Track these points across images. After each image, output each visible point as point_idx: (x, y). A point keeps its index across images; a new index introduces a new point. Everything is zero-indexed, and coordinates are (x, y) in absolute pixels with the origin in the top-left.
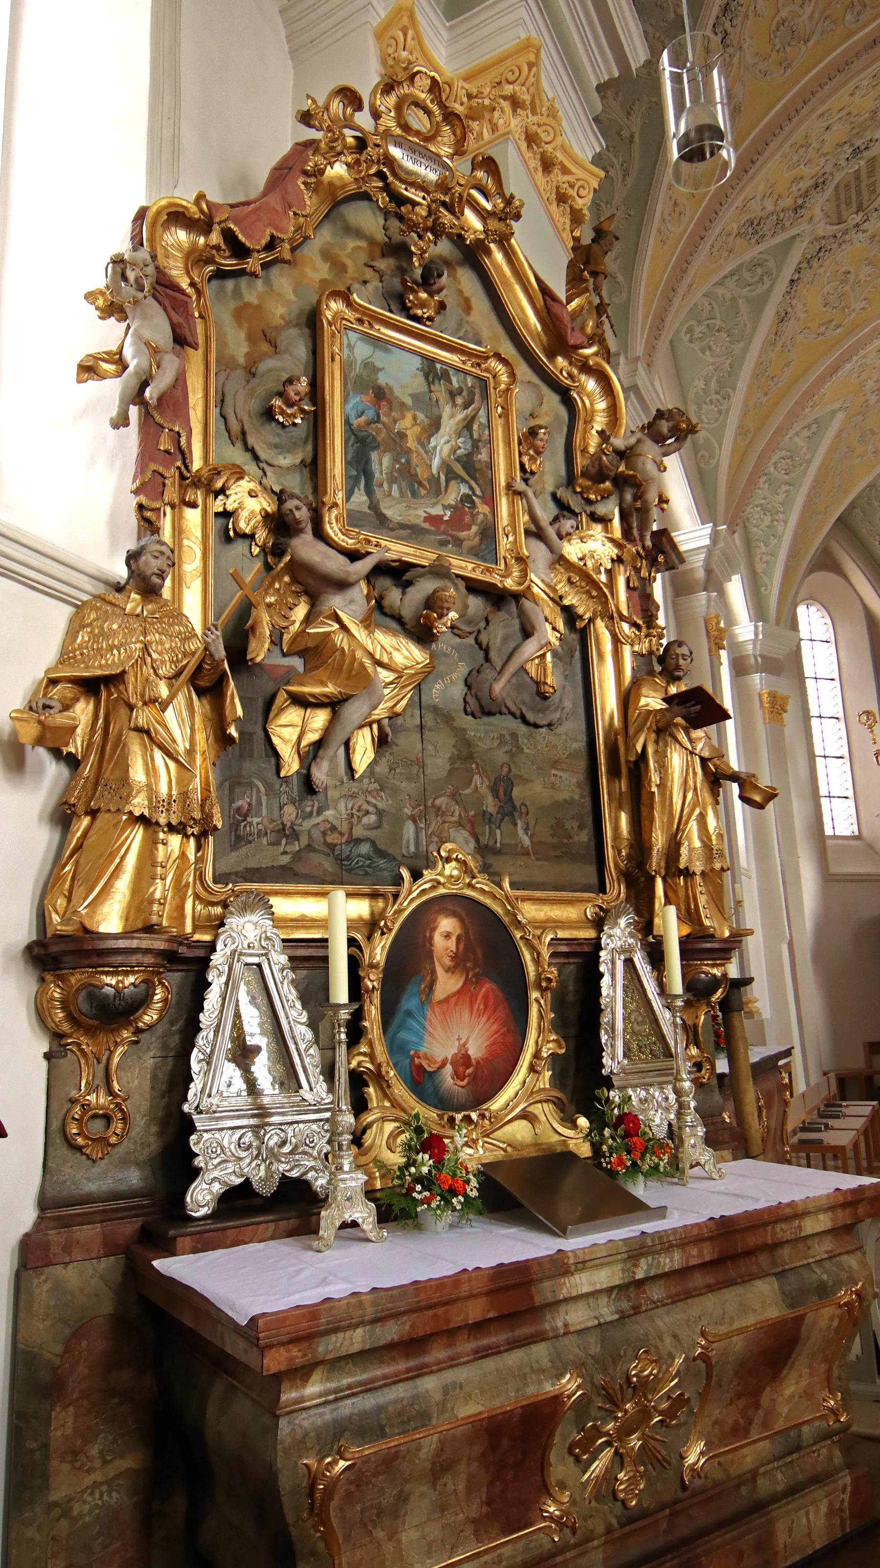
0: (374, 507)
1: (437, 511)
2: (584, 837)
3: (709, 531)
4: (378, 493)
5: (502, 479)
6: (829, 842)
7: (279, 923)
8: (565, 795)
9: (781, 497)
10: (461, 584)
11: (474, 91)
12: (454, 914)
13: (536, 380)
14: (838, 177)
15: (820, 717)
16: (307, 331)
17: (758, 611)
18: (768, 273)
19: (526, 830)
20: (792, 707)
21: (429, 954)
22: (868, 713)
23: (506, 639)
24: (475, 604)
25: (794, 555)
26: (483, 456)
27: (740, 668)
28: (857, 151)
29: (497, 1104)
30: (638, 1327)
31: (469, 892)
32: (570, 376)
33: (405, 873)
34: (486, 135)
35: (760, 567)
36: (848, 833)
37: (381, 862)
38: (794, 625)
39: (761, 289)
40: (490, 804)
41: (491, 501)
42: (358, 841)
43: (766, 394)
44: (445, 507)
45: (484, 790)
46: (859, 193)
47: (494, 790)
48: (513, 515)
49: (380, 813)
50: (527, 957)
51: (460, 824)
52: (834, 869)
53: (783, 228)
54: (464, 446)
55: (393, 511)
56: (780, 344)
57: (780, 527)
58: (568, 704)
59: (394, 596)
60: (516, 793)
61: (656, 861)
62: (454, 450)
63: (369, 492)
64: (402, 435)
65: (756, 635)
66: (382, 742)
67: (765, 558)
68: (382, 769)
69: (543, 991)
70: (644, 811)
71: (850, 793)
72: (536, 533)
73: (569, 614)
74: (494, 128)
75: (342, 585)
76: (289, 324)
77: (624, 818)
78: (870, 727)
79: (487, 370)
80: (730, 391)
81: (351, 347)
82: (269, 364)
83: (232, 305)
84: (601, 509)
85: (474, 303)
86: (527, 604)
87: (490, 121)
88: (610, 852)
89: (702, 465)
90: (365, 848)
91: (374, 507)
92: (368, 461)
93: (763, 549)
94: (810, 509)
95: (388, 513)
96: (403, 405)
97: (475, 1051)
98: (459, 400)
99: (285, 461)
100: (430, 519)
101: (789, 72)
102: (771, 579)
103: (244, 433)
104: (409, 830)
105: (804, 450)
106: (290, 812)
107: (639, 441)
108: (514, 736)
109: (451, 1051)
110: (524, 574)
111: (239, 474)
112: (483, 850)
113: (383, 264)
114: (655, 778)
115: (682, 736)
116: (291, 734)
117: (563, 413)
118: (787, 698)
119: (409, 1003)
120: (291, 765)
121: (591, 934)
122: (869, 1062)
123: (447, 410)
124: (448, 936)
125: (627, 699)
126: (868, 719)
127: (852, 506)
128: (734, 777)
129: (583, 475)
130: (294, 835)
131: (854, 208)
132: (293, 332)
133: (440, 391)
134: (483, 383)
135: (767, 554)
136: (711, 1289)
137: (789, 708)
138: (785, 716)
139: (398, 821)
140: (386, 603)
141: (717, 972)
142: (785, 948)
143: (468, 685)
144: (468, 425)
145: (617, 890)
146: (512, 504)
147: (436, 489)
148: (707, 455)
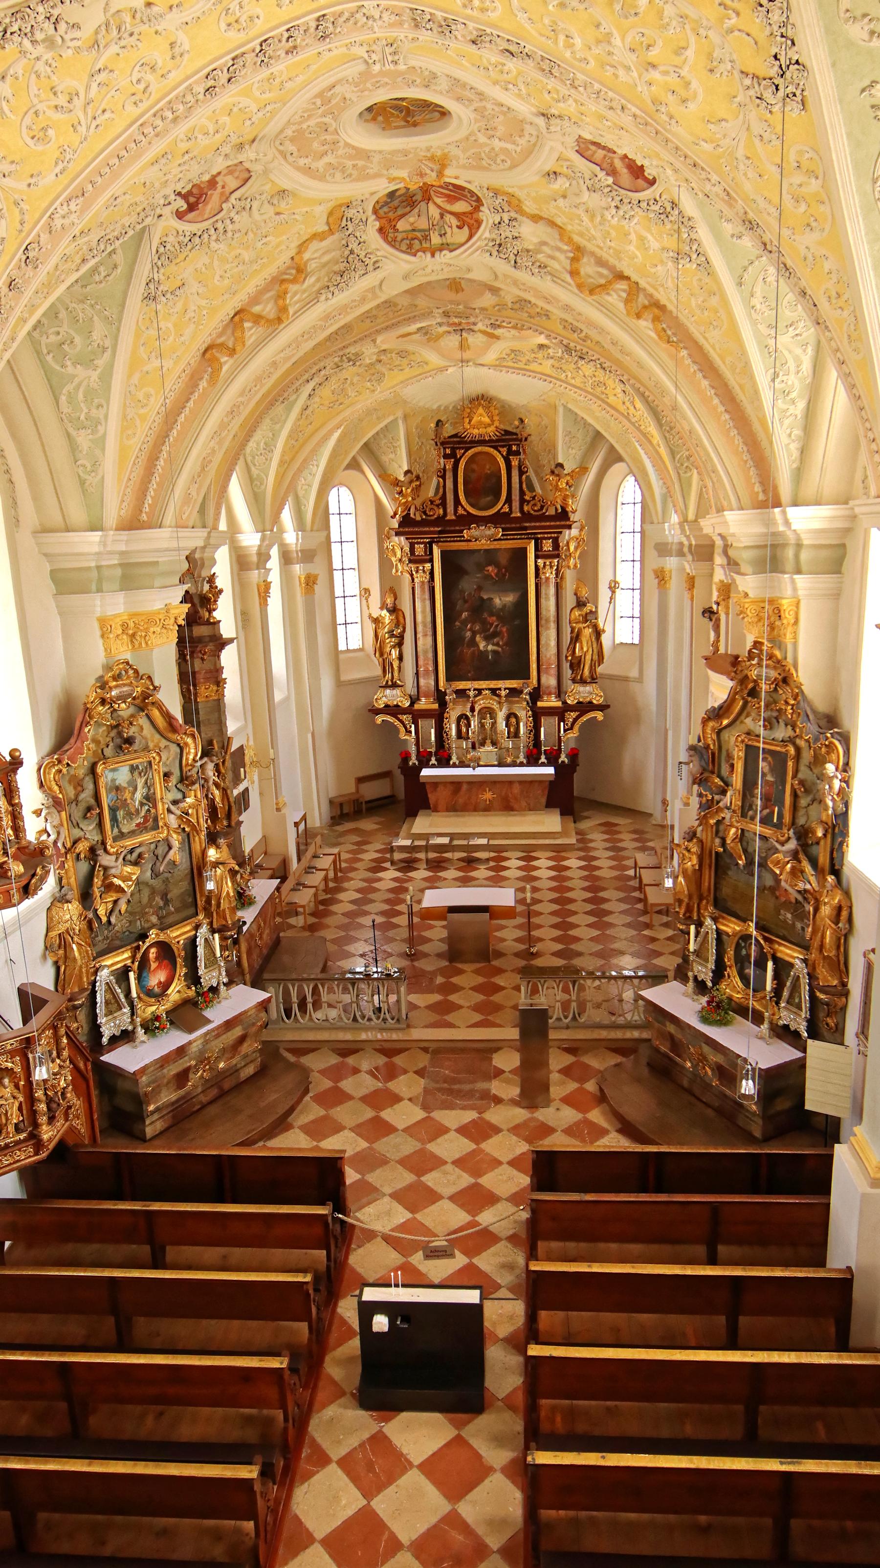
0: (120, 831)
5: (159, 796)
6: (341, 656)
13: (168, 743)
27: (286, 558)
29: (169, 992)
34: (144, 645)
40: (161, 904)
49: (130, 922)
54: (145, 790)
59: (129, 857)
61: (213, 908)
74: (147, 643)
76: (85, 775)
78: (367, 599)
82: (82, 796)
91: (120, 831)
99: (91, 828)
100: (138, 825)
109: (157, 981)
113: (113, 733)
117: (178, 750)
119: (145, 974)
120: (104, 919)
132: (87, 778)
133: (136, 773)
134: (150, 763)
139: (136, 921)
142: (310, 736)
144: (146, 783)
145: (201, 917)
147: (138, 812)
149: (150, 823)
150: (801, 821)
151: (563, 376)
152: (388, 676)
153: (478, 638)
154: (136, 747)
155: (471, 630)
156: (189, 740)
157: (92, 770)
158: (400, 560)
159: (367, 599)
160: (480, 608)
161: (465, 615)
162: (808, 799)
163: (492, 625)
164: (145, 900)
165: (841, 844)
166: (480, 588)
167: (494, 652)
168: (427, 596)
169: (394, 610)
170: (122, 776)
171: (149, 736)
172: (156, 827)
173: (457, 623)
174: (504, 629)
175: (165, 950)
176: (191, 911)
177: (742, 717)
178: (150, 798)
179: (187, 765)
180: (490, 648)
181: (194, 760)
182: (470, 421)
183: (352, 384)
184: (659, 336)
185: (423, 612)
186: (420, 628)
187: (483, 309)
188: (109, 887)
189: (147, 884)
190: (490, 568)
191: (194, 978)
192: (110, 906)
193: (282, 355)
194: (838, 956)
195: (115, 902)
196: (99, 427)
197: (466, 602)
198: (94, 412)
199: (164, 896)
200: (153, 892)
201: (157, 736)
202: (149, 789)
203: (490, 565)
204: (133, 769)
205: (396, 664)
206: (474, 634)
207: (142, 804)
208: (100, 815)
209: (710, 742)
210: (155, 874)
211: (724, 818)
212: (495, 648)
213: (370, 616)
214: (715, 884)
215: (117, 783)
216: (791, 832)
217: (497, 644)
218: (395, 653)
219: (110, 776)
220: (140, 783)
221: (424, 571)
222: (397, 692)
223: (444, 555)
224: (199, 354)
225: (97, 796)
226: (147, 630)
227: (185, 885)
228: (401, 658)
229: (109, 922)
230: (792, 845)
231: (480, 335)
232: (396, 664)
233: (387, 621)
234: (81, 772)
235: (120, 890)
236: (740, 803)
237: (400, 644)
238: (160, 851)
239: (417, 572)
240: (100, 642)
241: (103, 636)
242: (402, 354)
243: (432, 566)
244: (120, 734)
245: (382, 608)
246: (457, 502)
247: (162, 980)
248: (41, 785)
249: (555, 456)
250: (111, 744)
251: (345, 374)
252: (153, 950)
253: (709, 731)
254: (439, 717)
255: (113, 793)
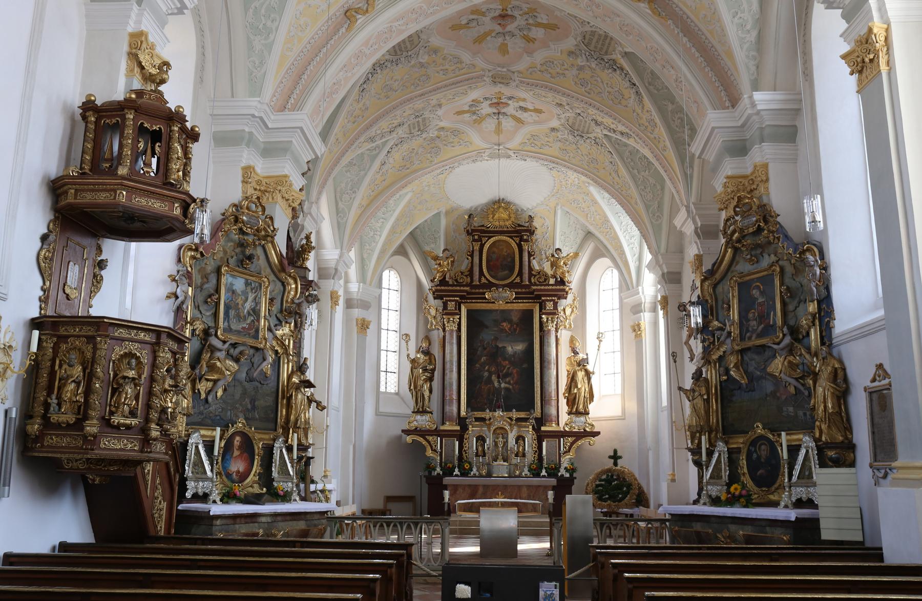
0: (229, 326)
1: (245, 325)
2: (272, 416)
3: (338, 252)
4: (230, 321)
7: (202, 436)
8: (269, 404)
9: (379, 225)
10: (249, 347)
11: (268, 183)
12: (240, 436)
13: (275, 279)
14: (409, 123)
15: (388, 330)
16: (216, 274)
17: (362, 279)
18: (379, 148)
19: (258, 413)
20: (373, 327)
21: (233, 446)
22: (407, 335)
23: (258, 360)
24: (252, 351)
25: (383, 251)
26: (258, 308)
27: (349, 304)
28: (417, 117)
30: (275, 524)
31: (244, 431)
32: (285, 278)
33: (230, 425)
34: (270, 199)
35: (365, 256)
36: (393, 391)
37: (222, 421)
38: (380, 285)
39: (374, 152)
40: (249, 406)
41: (258, 321)
42: (217, 416)
43: (373, 191)
44: (247, 324)
45: (248, 402)
46: (419, 126)
47: (251, 404)
48: (265, 325)
49: (223, 409)
50: (256, 448)
51: (241, 412)
52: (381, 410)
53: (385, 137)
55: (233, 327)
56: (381, 172)
57: (377, 238)
58: (273, 378)
59: (232, 351)
60: (256, 403)
62: (250, 307)
63: (228, 322)
64: (238, 304)
65: (359, 289)
66: (225, 390)
67: (369, 251)
68: (224, 397)
69: (258, 456)
70: (290, 410)
71: (396, 371)
72: (270, 330)
73: (276, 352)
74: (273, 198)
75: (220, 350)
76: (212, 272)
77: (284, 410)
78: (407, 342)
79: (263, 281)
80: (356, 189)
81: (227, 279)
82: (206, 286)
83: (198, 268)
84: (289, 321)
85: (260, 257)
86: (265, 351)
87: (272, 195)
88: (279, 420)
89: (339, 220)
90: (218, 418)
91: (229, 326)
92: (229, 313)
93: (368, 247)
94: (393, 231)
95: (232, 327)
96: (239, 295)
97: (241, 470)
98: (254, 291)
99: (208, 314)
100: (243, 328)
101: (388, 99)
102: (370, 262)
103: (198, 306)
104: (229, 413)
105: (393, 205)
106: (202, 408)
107: (302, 302)
108: (257, 387)
110: (266, 343)
111: (198, 319)
112: (246, 419)
113: (238, 250)
114: (294, 402)
115: (302, 390)
116: (204, 388)
118: (370, 322)
119: (228, 457)
120: (203, 396)
121: (271, 442)
122: (385, 505)
123: (250, 294)
124: (238, 441)
125: (290, 377)
126: (406, 338)
127: (416, 228)
128: (316, 401)
129: (286, 311)
130: (203, 414)
131: (417, 129)
132: (213, 275)
135: (370, 250)
136: (291, 520)
137: (370, 327)
138: (368, 330)
140: (230, 352)
141: (304, 455)
143: (247, 374)
144: (255, 299)
146: (265, 322)
147: (245, 319)
148: (342, 215)
149: (252, 332)
150: (792, 323)
151: (567, 158)
152: (420, 404)
153: (494, 377)
154: (252, 267)
155: (488, 371)
156: (291, 281)
157: (218, 271)
158: (435, 317)
159: (407, 342)
160: (496, 354)
161: (483, 359)
162: (796, 302)
163: (505, 367)
164: (237, 396)
165: (829, 322)
166: (496, 339)
167: (506, 389)
168: (455, 341)
169: (427, 353)
170: (239, 284)
171: (263, 267)
172: (256, 336)
173: (477, 365)
174: (515, 371)
175: (248, 446)
176: (272, 425)
177: (733, 268)
178: (255, 312)
179: (287, 301)
180: (503, 385)
181: (292, 300)
182: (493, 217)
183: (417, 153)
184: (653, 12)
185: (451, 353)
186: (448, 366)
187: (519, 72)
188: (212, 368)
189: (241, 383)
190: (505, 324)
191: (266, 479)
192: (210, 384)
193: (396, 24)
194: (840, 414)
195: (215, 382)
196: (270, 35)
197: (485, 349)
198: (269, 23)
199: (253, 401)
200: (245, 393)
201: (268, 270)
202: (256, 305)
203: (504, 321)
204: (247, 284)
205: (427, 394)
206: (491, 374)
207: (249, 314)
208: (217, 304)
209: (708, 298)
210: (250, 380)
211: (724, 352)
212: (507, 385)
213: (408, 355)
214: (722, 414)
215: (234, 288)
216: (785, 329)
217: (509, 383)
218: (426, 387)
219: (230, 279)
220: (251, 297)
221: (454, 322)
222: (426, 417)
223: (470, 313)
224: (342, 11)
225: (217, 290)
226: (275, 189)
227: (270, 401)
228: (431, 391)
229: (206, 400)
230: (788, 340)
231: (510, 119)
232: (427, 394)
233: (421, 361)
234: (209, 268)
235: (221, 372)
236: (737, 332)
237: (431, 379)
238: (256, 359)
239: (448, 322)
240: (240, 185)
241: (243, 182)
242: (456, 132)
243: (460, 319)
244: (243, 252)
245: (418, 352)
246: (481, 273)
247: (241, 470)
248: (179, 261)
249: (554, 244)
250: (235, 257)
251: (416, 143)
252: (238, 438)
253: (706, 287)
254: (461, 436)
255: (230, 294)
